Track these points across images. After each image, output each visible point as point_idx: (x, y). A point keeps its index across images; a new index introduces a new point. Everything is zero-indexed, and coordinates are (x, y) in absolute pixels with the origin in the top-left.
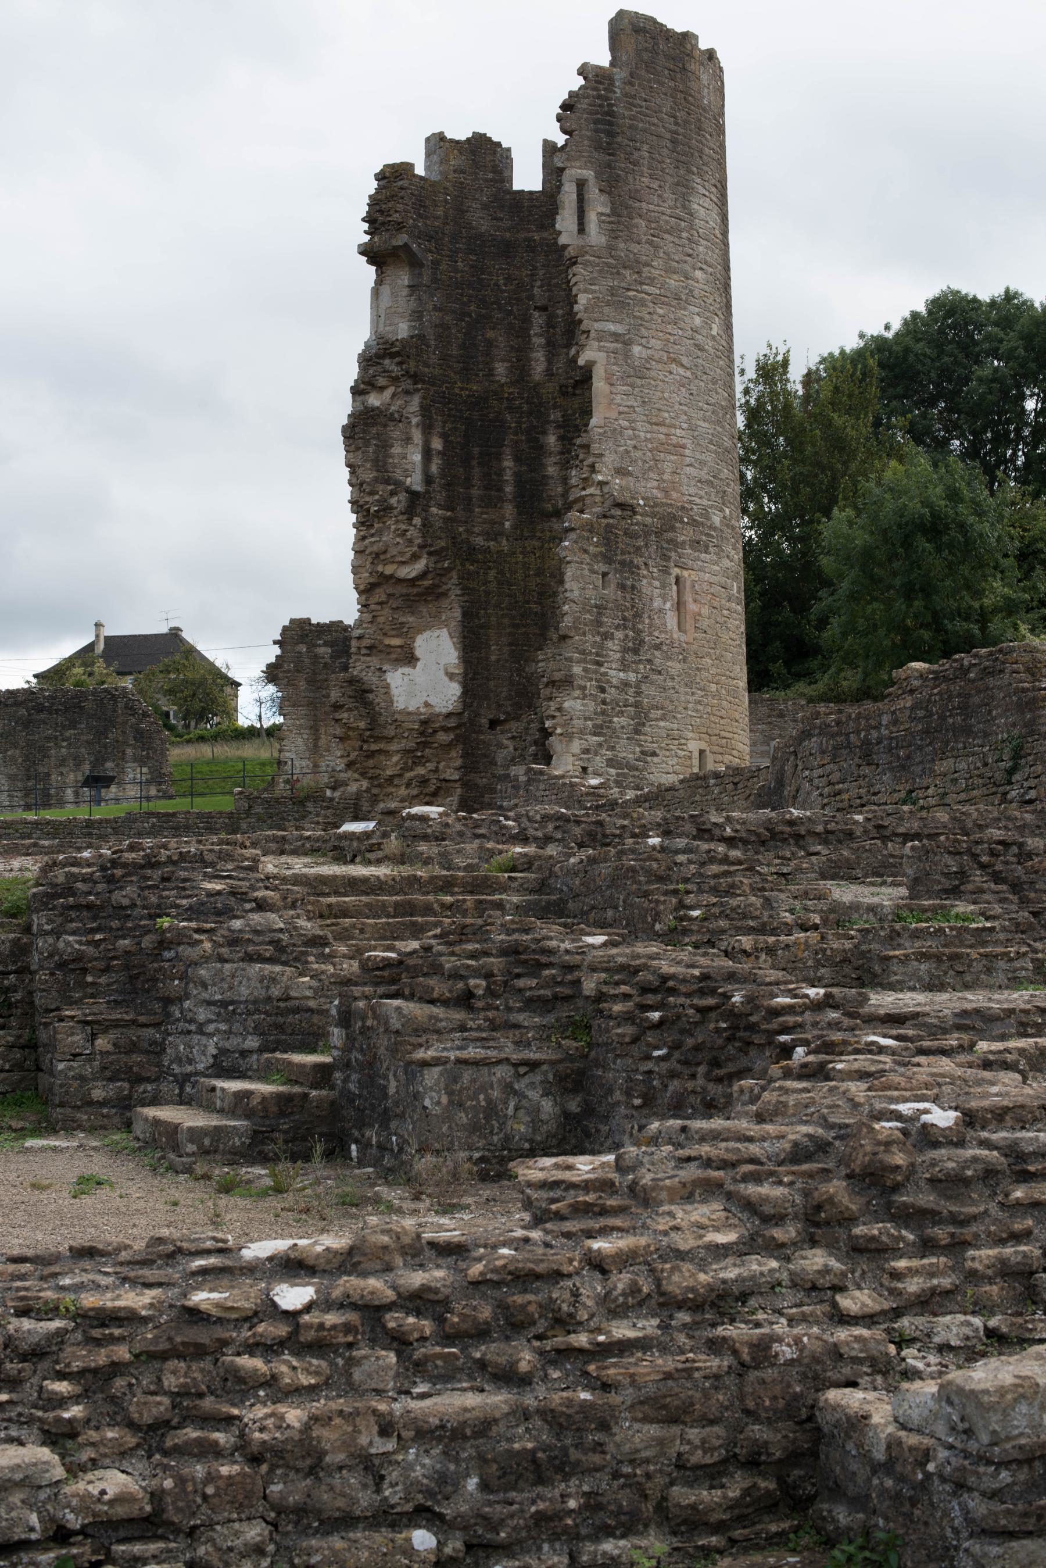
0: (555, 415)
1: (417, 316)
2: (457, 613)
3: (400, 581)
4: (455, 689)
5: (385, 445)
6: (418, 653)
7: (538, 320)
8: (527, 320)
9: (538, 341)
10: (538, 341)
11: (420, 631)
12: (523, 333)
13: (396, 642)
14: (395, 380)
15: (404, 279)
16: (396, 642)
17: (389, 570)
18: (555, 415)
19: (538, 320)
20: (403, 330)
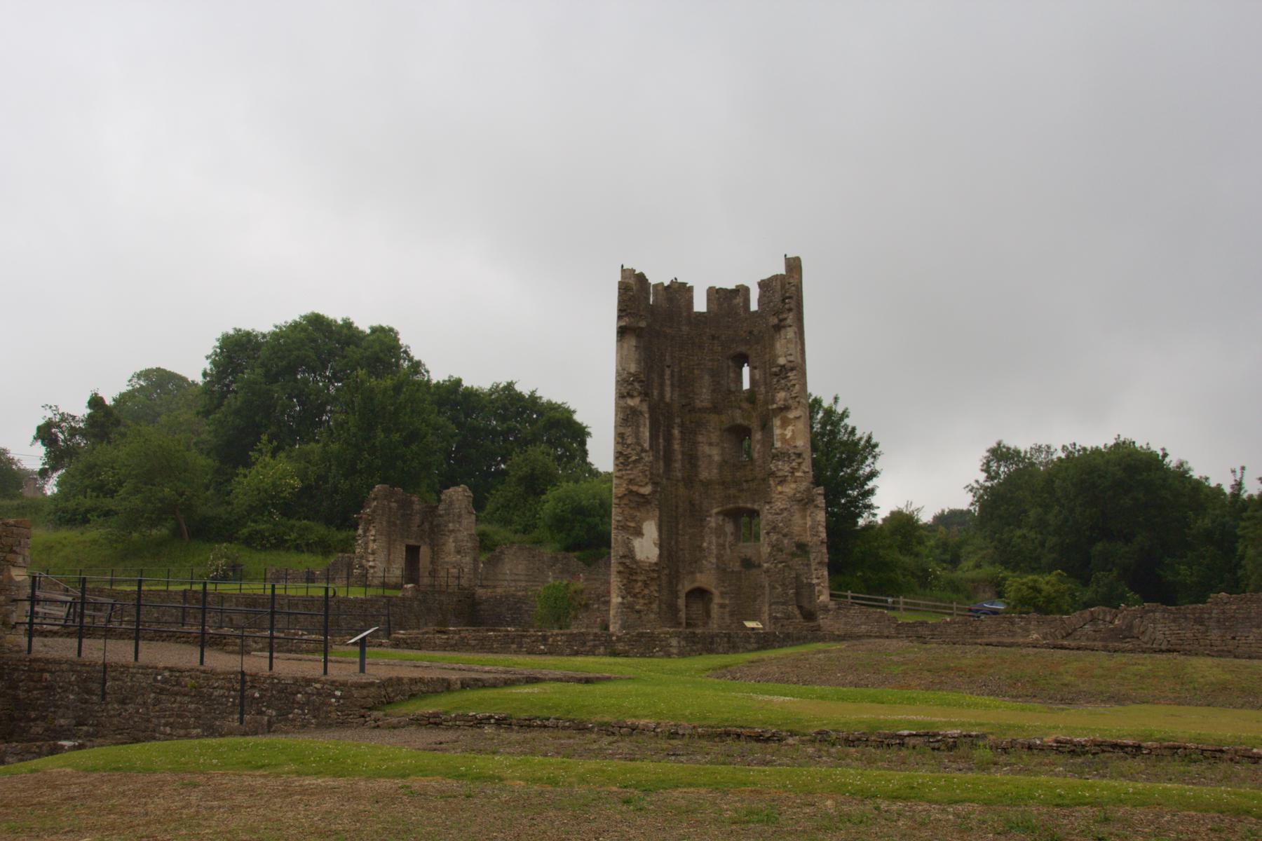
0: (678, 420)
1: (638, 362)
2: (657, 513)
3: (638, 494)
4: (656, 551)
5: (638, 427)
6: (645, 531)
7: (668, 372)
8: (663, 371)
9: (668, 382)
10: (668, 382)
11: (644, 520)
12: (661, 376)
13: (632, 524)
14: (640, 394)
15: (633, 342)
16: (632, 524)
17: (635, 488)
18: (678, 420)
19: (668, 372)
20: (633, 368)
